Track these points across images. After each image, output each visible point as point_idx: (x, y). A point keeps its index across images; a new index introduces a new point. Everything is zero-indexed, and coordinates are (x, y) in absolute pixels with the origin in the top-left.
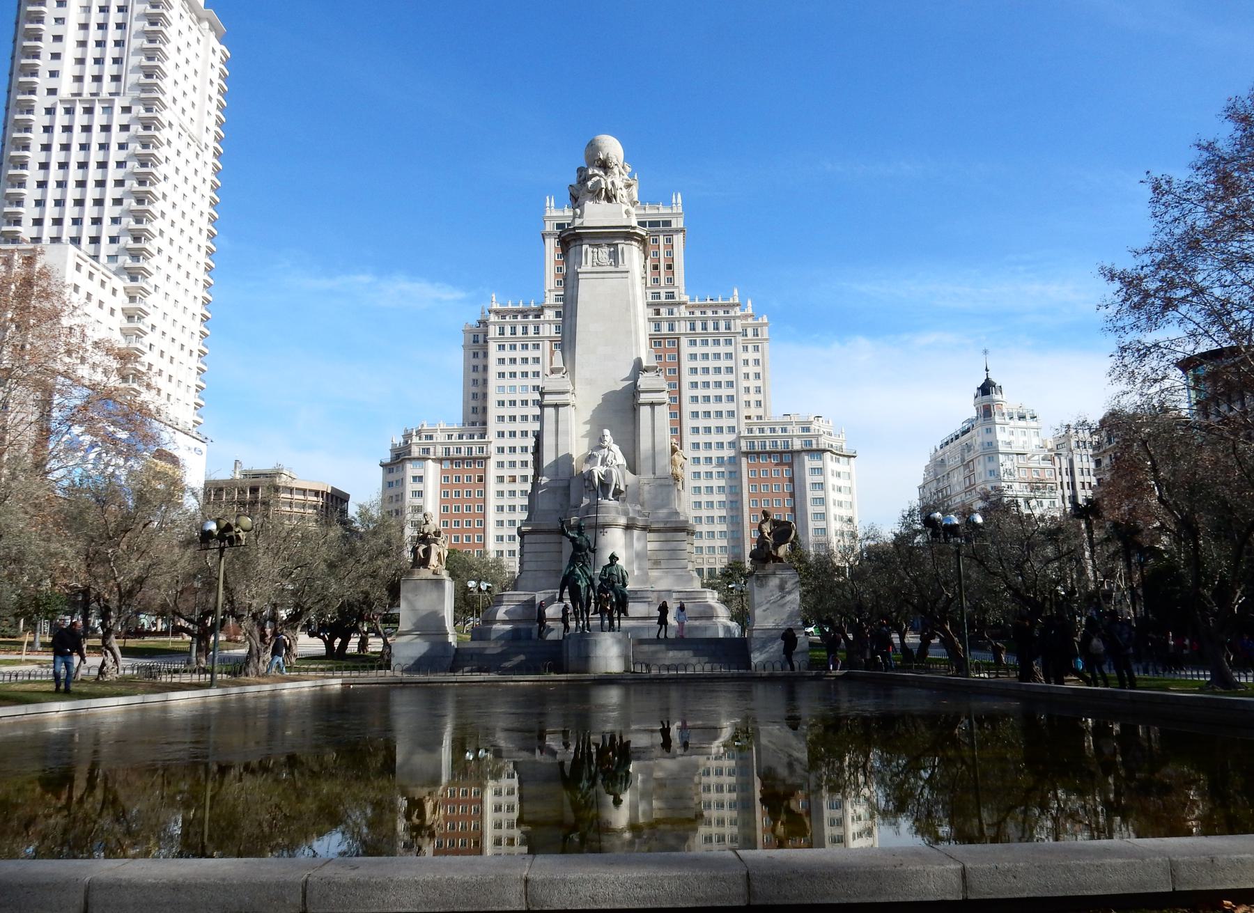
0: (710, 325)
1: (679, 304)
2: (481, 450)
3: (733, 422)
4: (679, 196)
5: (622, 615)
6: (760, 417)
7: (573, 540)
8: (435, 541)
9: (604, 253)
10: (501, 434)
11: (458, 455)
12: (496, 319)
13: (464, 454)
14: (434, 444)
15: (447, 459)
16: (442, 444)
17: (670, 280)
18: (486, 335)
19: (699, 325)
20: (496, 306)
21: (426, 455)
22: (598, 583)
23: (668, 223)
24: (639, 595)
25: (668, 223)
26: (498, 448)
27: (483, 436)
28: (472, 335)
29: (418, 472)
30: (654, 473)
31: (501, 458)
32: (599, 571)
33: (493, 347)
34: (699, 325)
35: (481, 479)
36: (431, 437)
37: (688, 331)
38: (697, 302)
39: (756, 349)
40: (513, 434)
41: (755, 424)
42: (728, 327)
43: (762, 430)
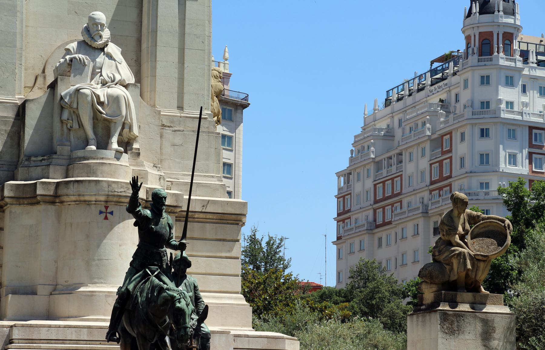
30: (180, 108)
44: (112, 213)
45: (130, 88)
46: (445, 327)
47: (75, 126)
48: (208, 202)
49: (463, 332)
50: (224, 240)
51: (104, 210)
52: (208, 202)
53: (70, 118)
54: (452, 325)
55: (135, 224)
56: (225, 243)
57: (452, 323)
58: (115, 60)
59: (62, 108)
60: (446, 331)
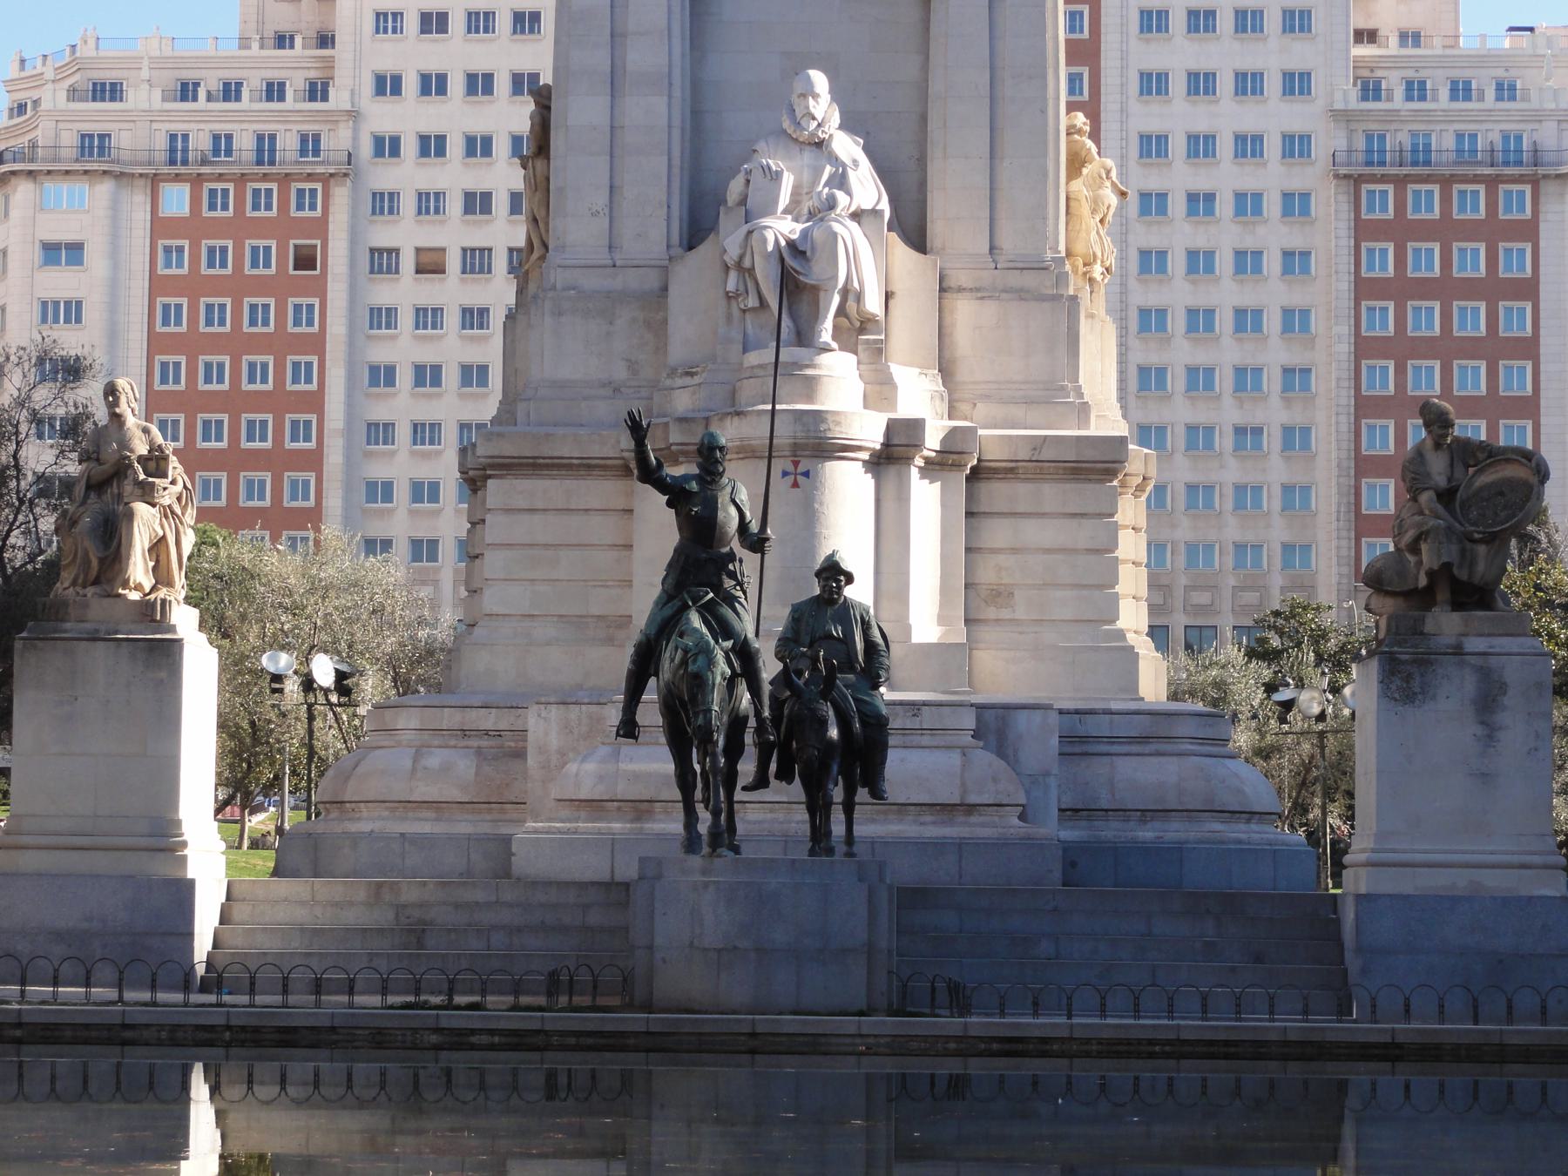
2: (310, 144)
3: (1300, 53)
5: (862, 794)
8: (147, 493)
10: (388, 85)
15: (177, 178)
22: (770, 668)
24: (928, 719)
26: (379, 141)
27: (317, 91)
31: (386, 177)
32: (777, 620)
35: (305, 260)
40: (433, 85)
41: (1394, 63)
44: (806, 474)
45: (865, 220)
46: (1393, 687)
47: (752, 301)
48: (1045, 441)
49: (1434, 698)
50: (1083, 515)
51: (791, 468)
52: (1045, 441)
53: (742, 288)
54: (1408, 682)
55: (669, 504)
56: (1084, 521)
57: (1408, 678)
58: (844, 166)
59: (727, 268)
60: (1397, 696)
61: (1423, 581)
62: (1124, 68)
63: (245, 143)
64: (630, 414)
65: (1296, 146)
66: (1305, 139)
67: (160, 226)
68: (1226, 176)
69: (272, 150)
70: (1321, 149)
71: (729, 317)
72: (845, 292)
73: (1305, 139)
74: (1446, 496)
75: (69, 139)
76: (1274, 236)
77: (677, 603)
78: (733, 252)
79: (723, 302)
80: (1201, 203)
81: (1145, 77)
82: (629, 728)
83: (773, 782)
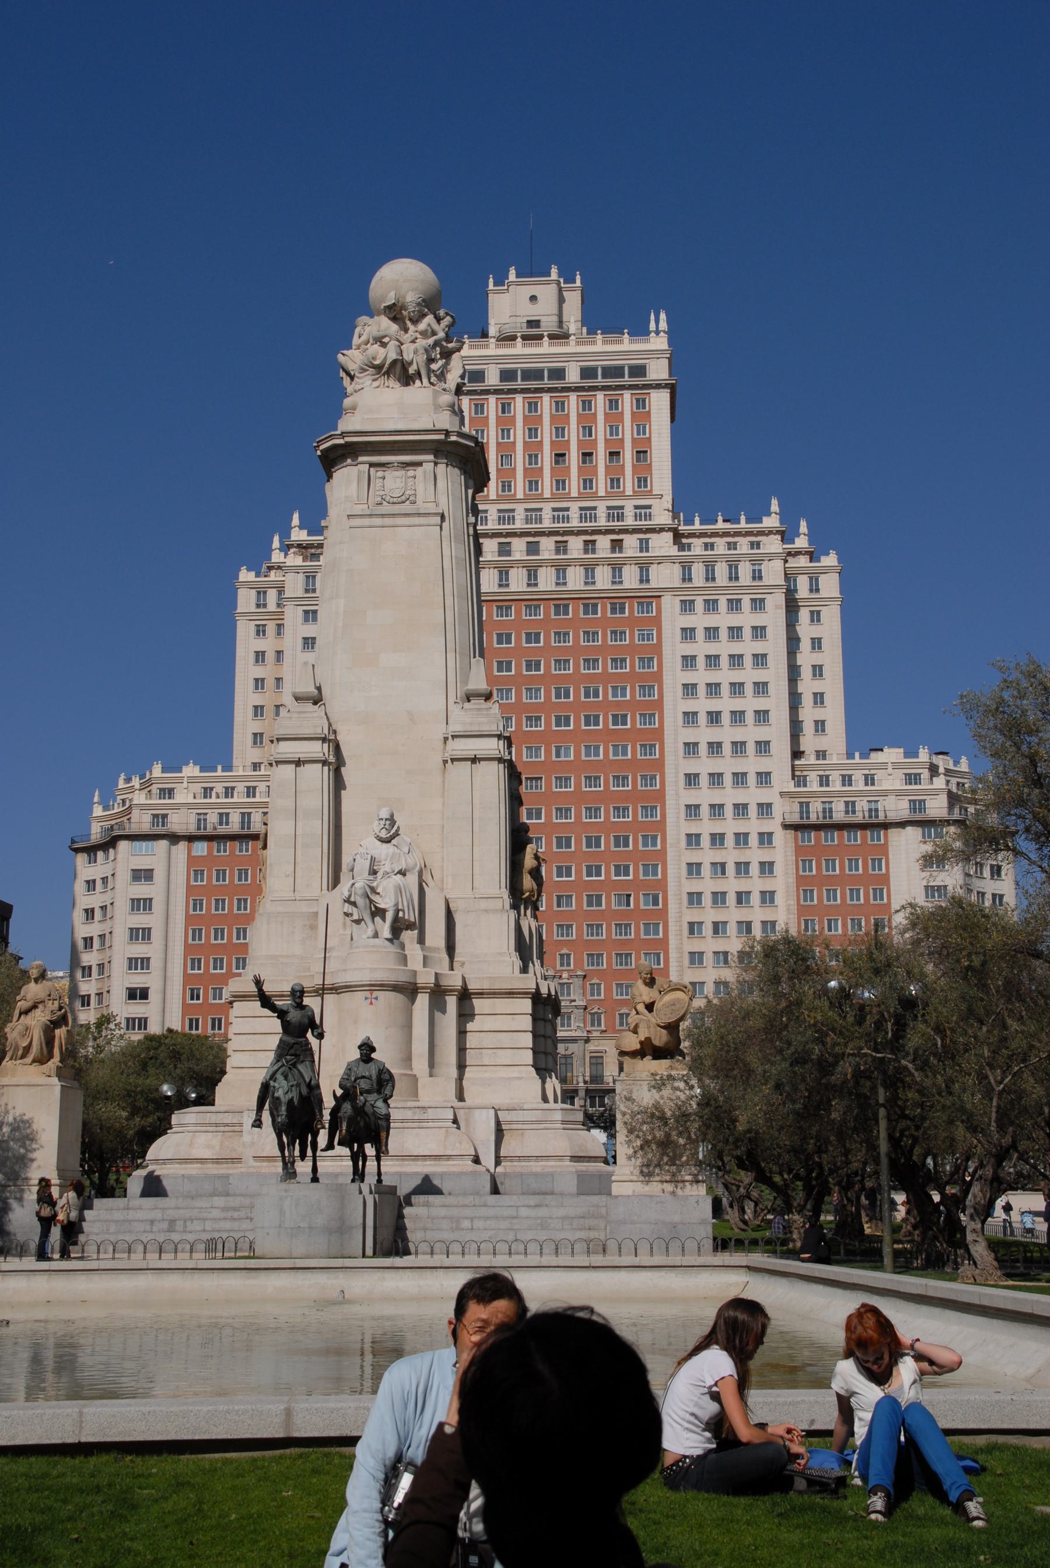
0: (721, 571)
1: (662, 530)
4: (663, 316)
6: (821, 754)
7: (282, 1014)
9: (394, 481)
11: (223, 830)
12: (298, 561)
13: (234, 825)
14: (177, 807)
16: (189, 806)
17: (642, 482)
18: (281, 590)
19: (698, 571)
20: (299, 535)
21: (160, 830)
23: (639, 371)
25: (639, 371)
28: (254, 592)
29: (142, 863)
33: (293, 615)
34: (698, 571)
36: (169, 793)
37: (677, 583)
38: (697, 526)
39: (815, 617)
42: (757, 576)
43: (824, 780)
44: (376, 998)
61: (638, 1047)
62: (677, 773)
63: (235, 818)
64: (255, 976)
65: (765, 809)
66: (769, 805)
67: (191, 860)
68: (730, 826)
69: (249, 822)
70: (778, 811)
71: (344, 925)
72: (397, 911)
73: (769, 805)
74: (650, 1007)
75: (147, 818)
76: (755, 855)
77: (280, 1064)
78: (346, 894)
79: (342, 916)
80: (718, 839)
81: (688, 776)
82: (258, 1123)
83: (337, 1147)
